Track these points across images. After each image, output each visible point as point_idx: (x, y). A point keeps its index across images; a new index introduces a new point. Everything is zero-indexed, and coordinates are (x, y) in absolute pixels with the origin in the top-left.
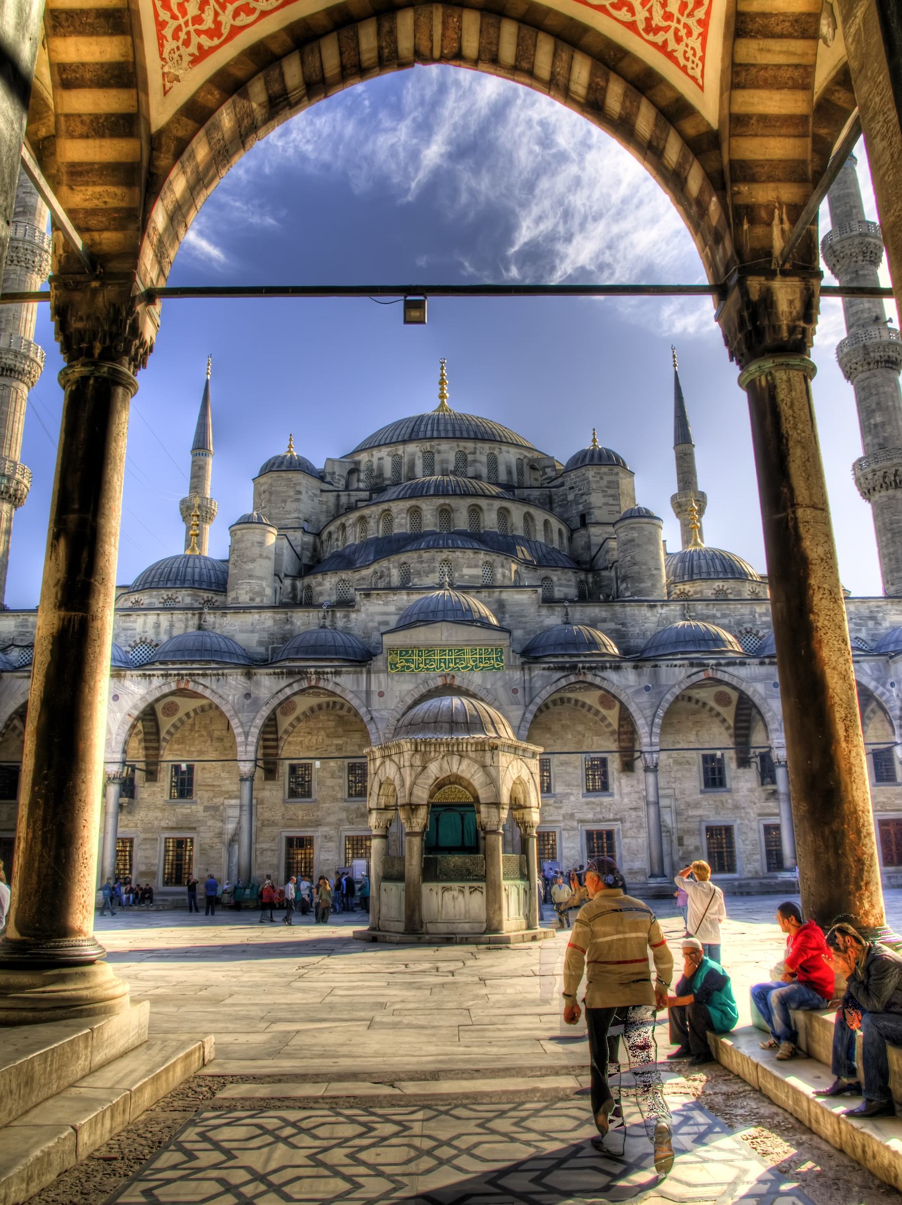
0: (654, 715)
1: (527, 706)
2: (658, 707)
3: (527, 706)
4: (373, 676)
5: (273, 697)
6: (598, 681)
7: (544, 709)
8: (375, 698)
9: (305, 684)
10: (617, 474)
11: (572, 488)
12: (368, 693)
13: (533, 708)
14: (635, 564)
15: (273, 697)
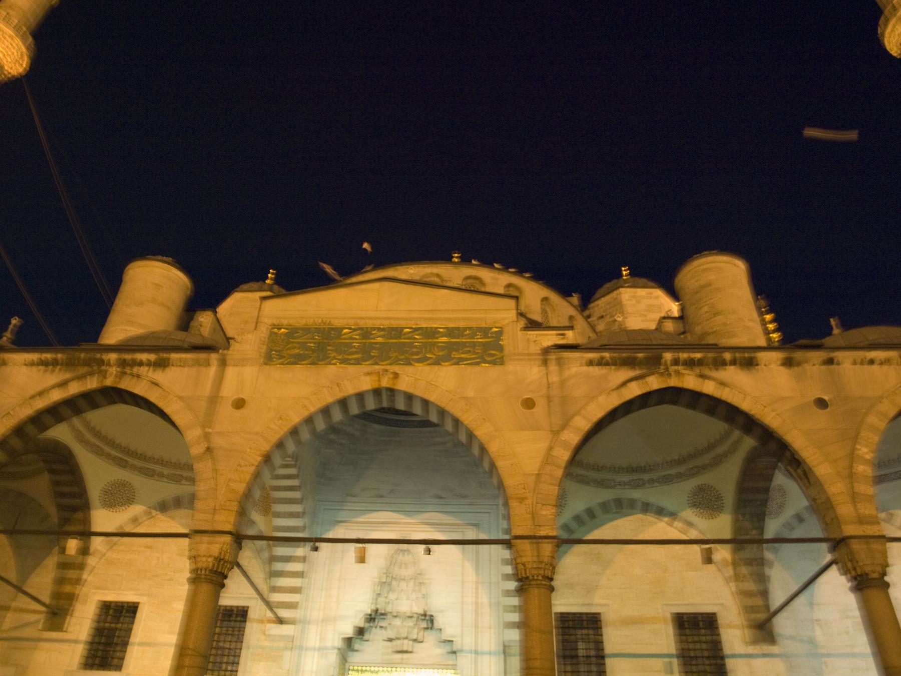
0: (852, 456)
1: (556, 433)
2: (856, 439)
3: (556, 433)
4: (230, 371)
5: (21, 405)
6: (709, 388)
7: (586, 518)
8: (225, 410)
9: (92, 384)
10: (657, 297)
11: (602, 317)
12: (214, 400)
13: (572, 438)
14: (717, 314)
15: (21, 405)
